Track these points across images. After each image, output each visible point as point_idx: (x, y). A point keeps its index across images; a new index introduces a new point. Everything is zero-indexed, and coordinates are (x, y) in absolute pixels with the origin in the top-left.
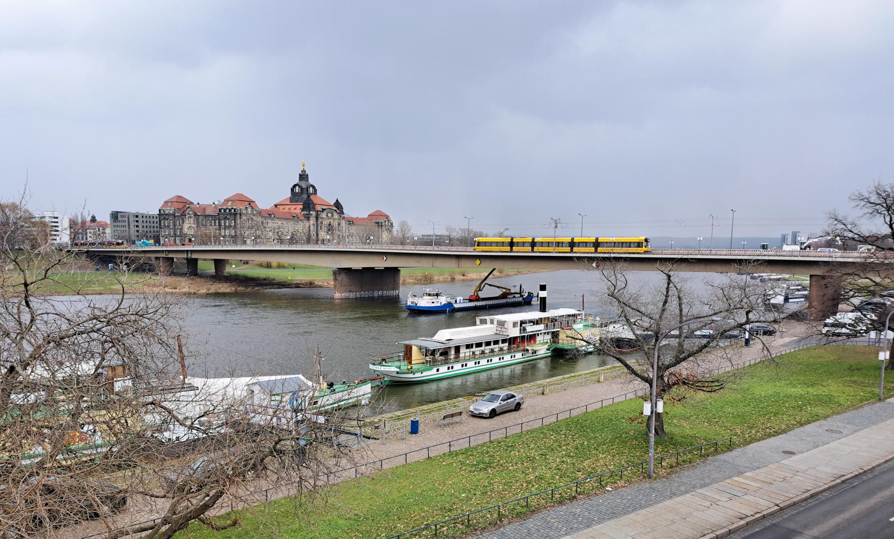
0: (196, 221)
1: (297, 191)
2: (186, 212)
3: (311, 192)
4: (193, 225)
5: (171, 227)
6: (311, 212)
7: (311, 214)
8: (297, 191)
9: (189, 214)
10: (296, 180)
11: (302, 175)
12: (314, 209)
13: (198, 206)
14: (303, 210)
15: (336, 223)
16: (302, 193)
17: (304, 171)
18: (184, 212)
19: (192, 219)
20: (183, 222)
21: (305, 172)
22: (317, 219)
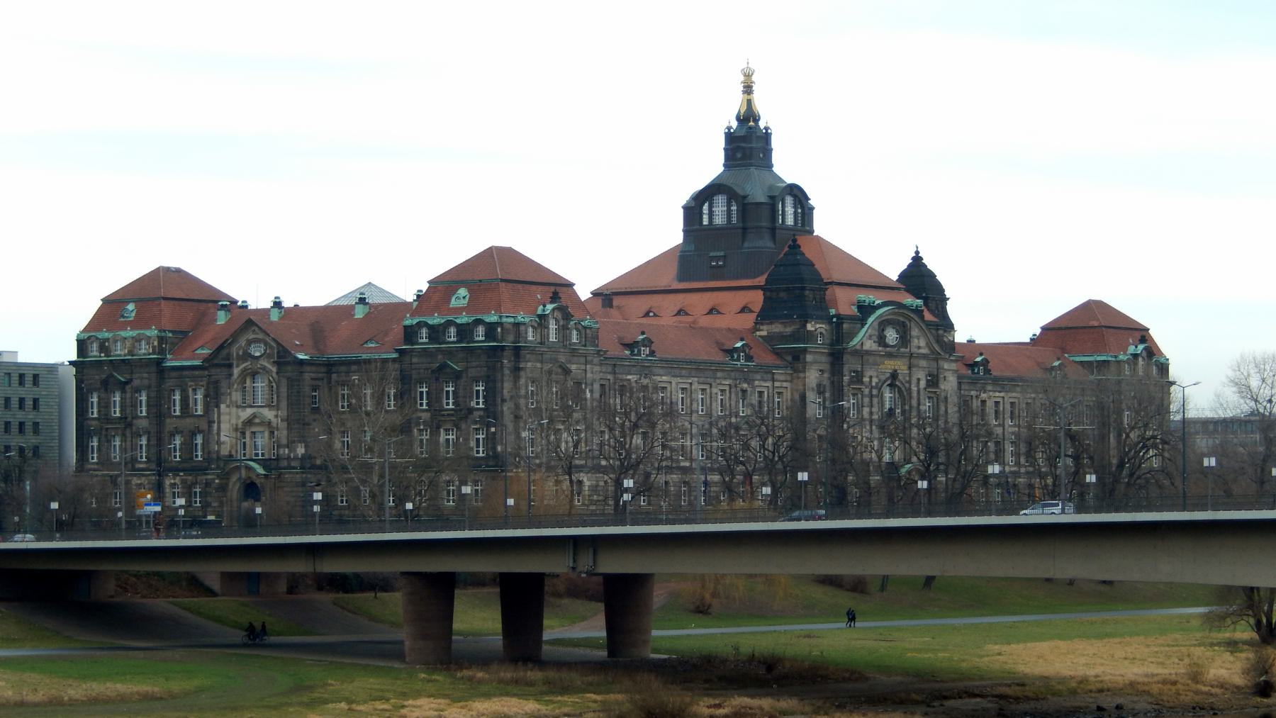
0: (284, 390)
1: (719, 220)
2: (234, 350)
3: (790, 221)
4: (269, 414)
5: (143, 423)
6: (810, 327)
7: (810, 337)
8: (719, 220)
9: (247, 356)
11: (743, 139)
12: (821, 309)
13: (275, 316)
14: (766, 315)
15: (921, 375)
16: (744, 229)
17: (748, 117)
18: (221, 347)
19: (261, 384)
20: (214, 398)
21: (756, 120)
22: (837, 357)
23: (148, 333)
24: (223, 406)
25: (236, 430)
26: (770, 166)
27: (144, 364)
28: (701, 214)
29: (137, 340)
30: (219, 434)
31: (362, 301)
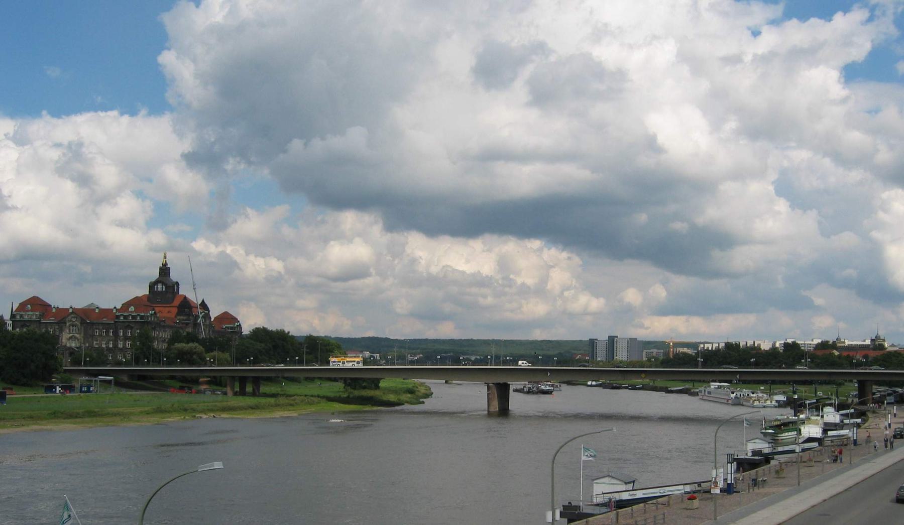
8: (160, 289)
10: (156, 274)
17: (165, 265)
23: (36, 313)
24: (63, 333)
25: (67, 339)
26: (170, 277)
27: (35, 321)
28: (154, 288)
29: (33, 315)
30: (62, 339)
31: (71, 307)
